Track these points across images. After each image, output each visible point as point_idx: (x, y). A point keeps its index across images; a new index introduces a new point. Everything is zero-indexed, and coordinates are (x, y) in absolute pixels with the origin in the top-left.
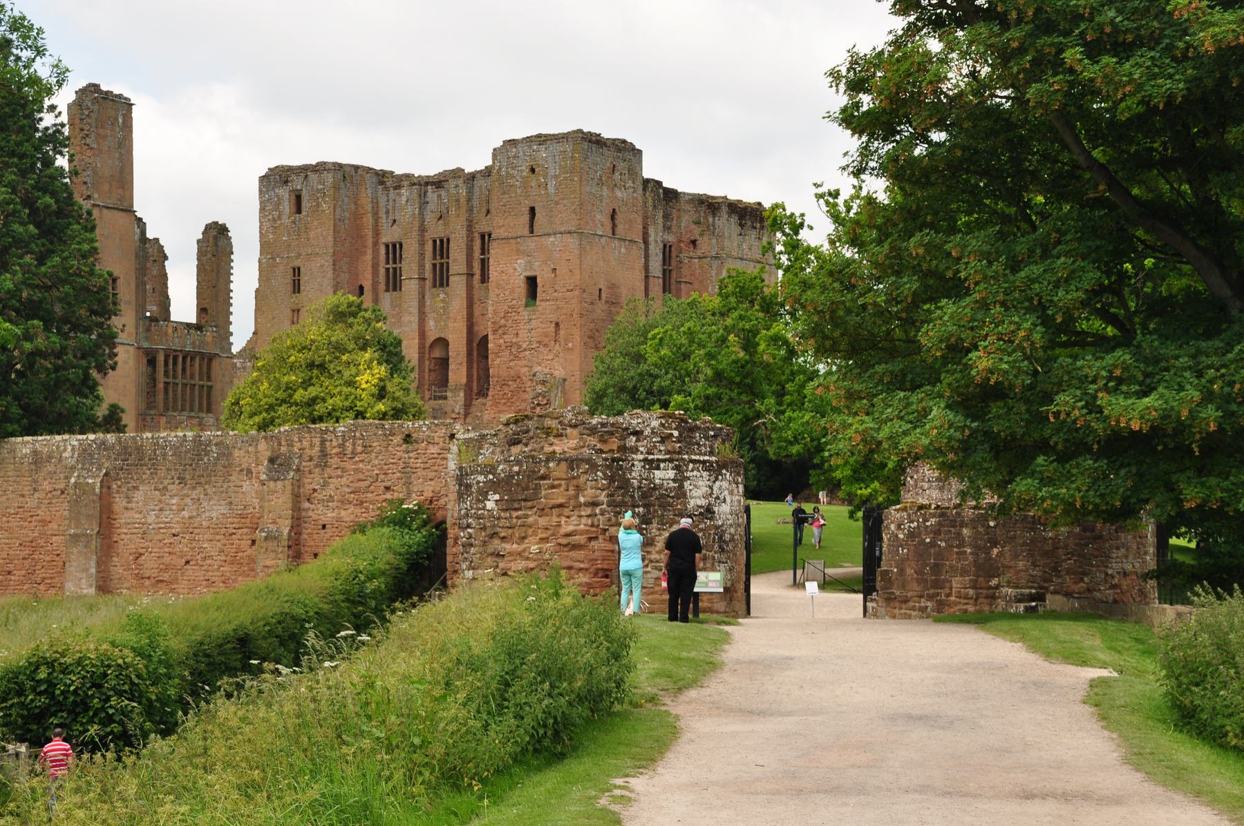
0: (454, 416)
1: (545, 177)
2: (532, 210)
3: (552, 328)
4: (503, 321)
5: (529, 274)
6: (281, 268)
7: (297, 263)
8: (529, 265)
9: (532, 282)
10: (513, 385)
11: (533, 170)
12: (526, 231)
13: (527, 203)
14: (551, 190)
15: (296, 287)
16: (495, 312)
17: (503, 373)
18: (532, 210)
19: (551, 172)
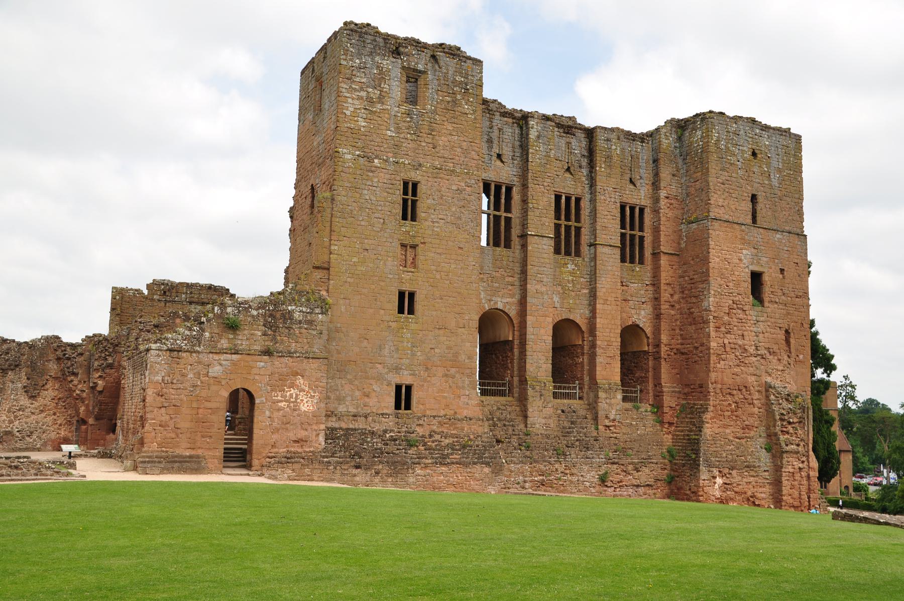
0: (607, 423)
1: (769, 165)
2: (754, 198)
3: (782, 336)
4: (726, 318)
5: (757, 268)
6: (383, 176)
7: (414, 176)
8: (756, 258)
9: (756, 278)
10: (738, 396)
11: (754, 154)
12: (749, 220)
13: (749, 190)
14: (775, 183)
15: (409, 211)
16: (718, 306)
17: (728, 380)
18: (754, 198)
19: (774, 164)
